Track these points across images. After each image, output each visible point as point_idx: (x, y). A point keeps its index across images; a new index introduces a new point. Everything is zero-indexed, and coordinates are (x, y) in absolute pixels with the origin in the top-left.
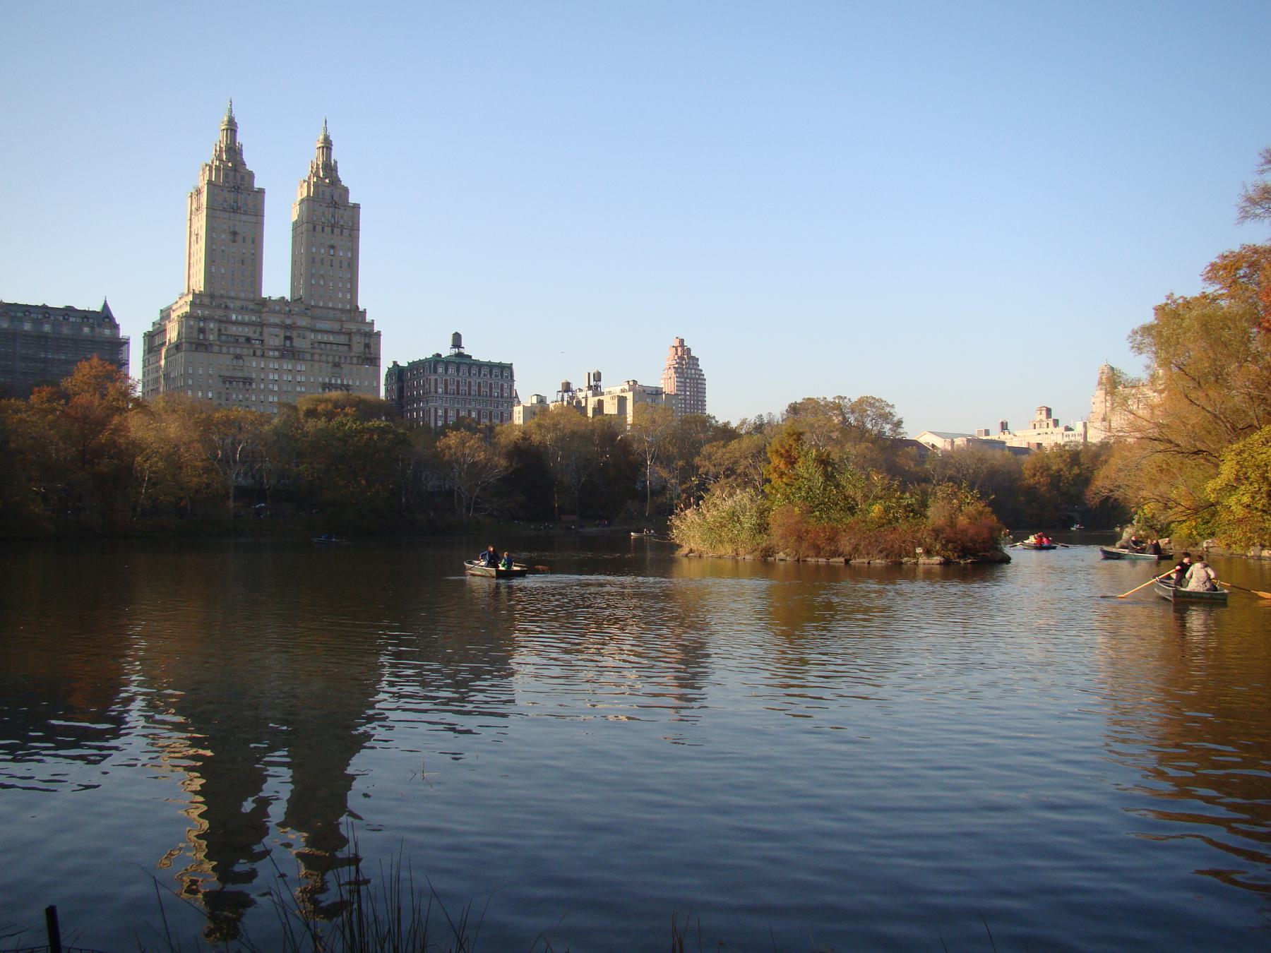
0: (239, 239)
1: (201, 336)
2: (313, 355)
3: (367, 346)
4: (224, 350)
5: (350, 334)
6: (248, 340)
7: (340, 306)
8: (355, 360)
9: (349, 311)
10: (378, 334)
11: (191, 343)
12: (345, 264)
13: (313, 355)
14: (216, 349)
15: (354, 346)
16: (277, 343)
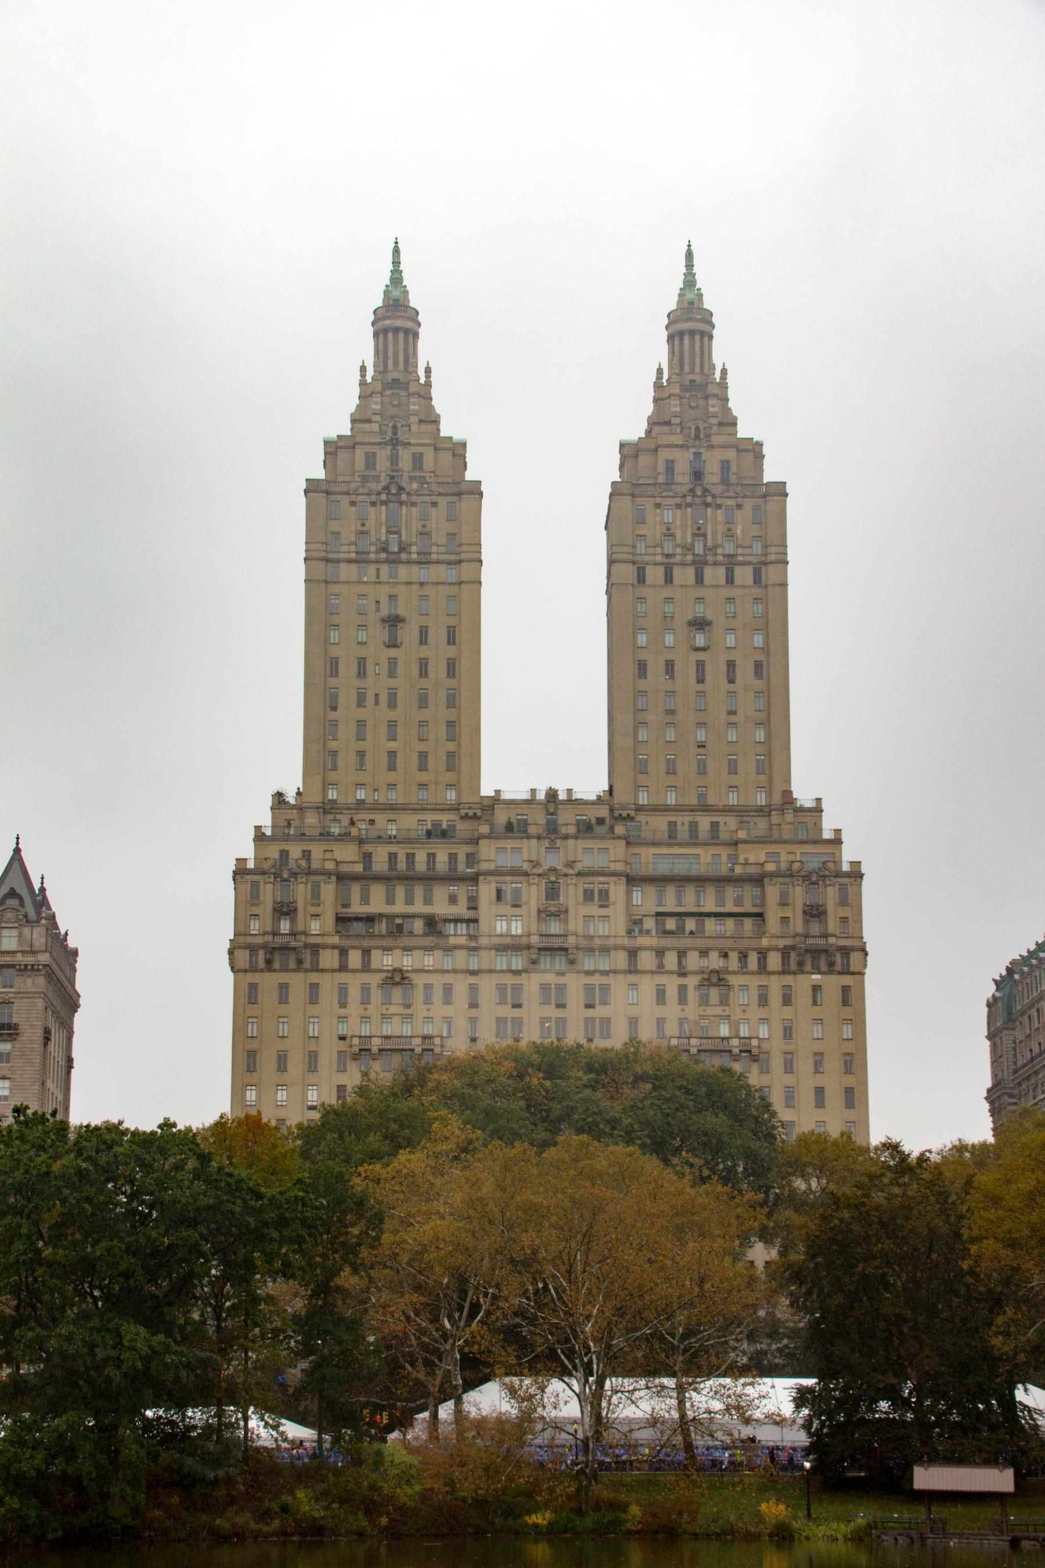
0: (408, 634)
1: (285, 926)
2: (633, 954)
3: (815, 913)
4: (355, 959)
5: (758, 880)
6: (432, 924)
7: (733, 799)
8: (774, 961)
9: (764, 812)
10: (856, 874)
11: (252, 949)
12: (745, 671)
13: (633, 954)
14: (329, 959)
15: (773, 915)
16: (517, 928)
